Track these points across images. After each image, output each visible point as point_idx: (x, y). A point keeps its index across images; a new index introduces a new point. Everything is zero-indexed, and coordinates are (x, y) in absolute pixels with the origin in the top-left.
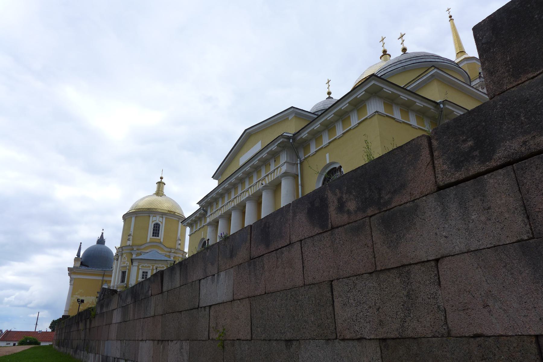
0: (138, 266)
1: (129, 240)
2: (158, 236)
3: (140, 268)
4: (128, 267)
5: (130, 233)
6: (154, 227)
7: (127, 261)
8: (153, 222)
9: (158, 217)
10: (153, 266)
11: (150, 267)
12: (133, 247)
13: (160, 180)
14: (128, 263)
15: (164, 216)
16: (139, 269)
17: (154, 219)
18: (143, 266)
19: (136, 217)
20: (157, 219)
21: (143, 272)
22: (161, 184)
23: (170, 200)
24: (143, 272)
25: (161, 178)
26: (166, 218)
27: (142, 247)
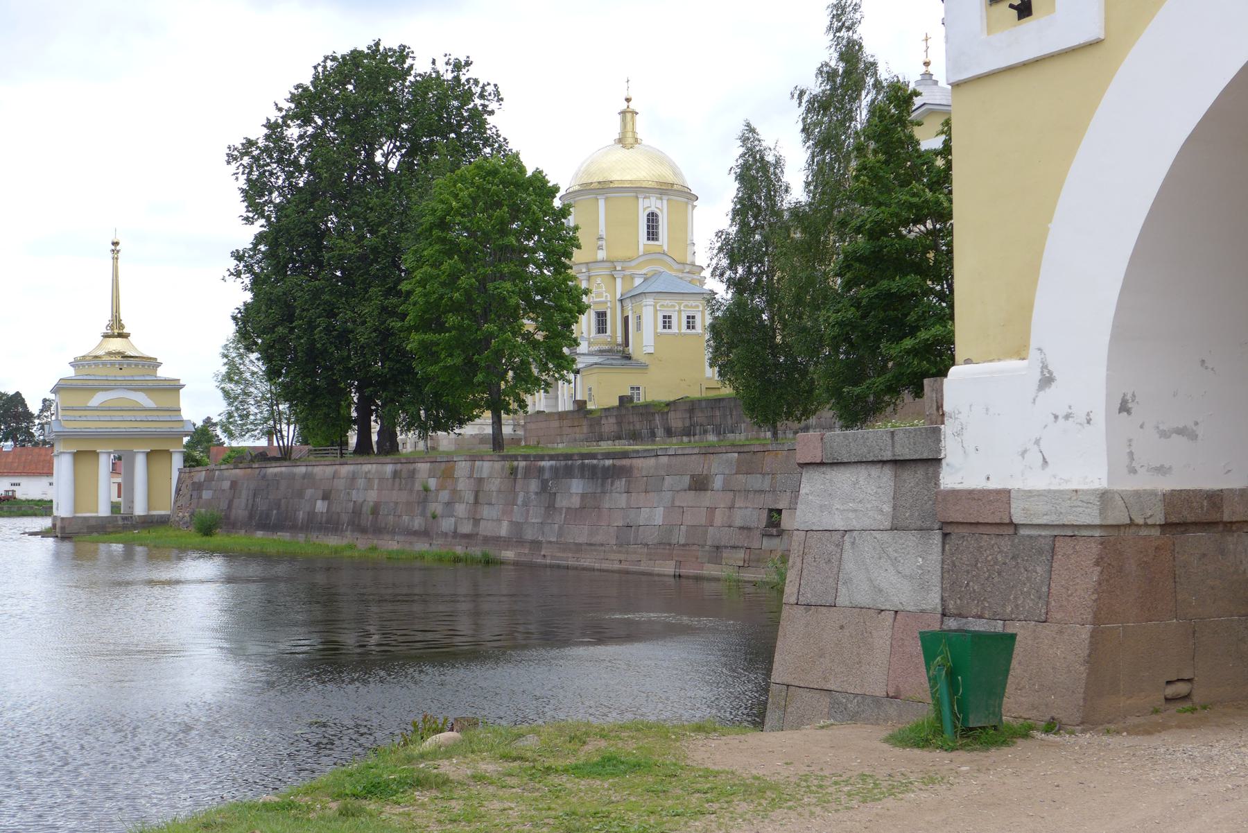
0: (655, 306)
1: (600, 248)
2: (657, 239)
3: (658, 308)
4: (609, 304)
5: (600, 233)
6: (648, 220)
7: (606, 292)
8: (645, 209)
9: (653, 199)
10: (680, 304)
11: (673, 306)
12: (616, 264)
13: (624, 105)
14: (609, 295)
15: (665, 197)
16: (656, 311)
17: (647, 202)
18: (686, 306)
19: (606, 199)
20: (652, 204)
21: (665, 317)
22: (627, 115)
23: (660, 158)
24: (665, 317)
25: (628, 100)
26: (668, 200)
27: (633, 264)
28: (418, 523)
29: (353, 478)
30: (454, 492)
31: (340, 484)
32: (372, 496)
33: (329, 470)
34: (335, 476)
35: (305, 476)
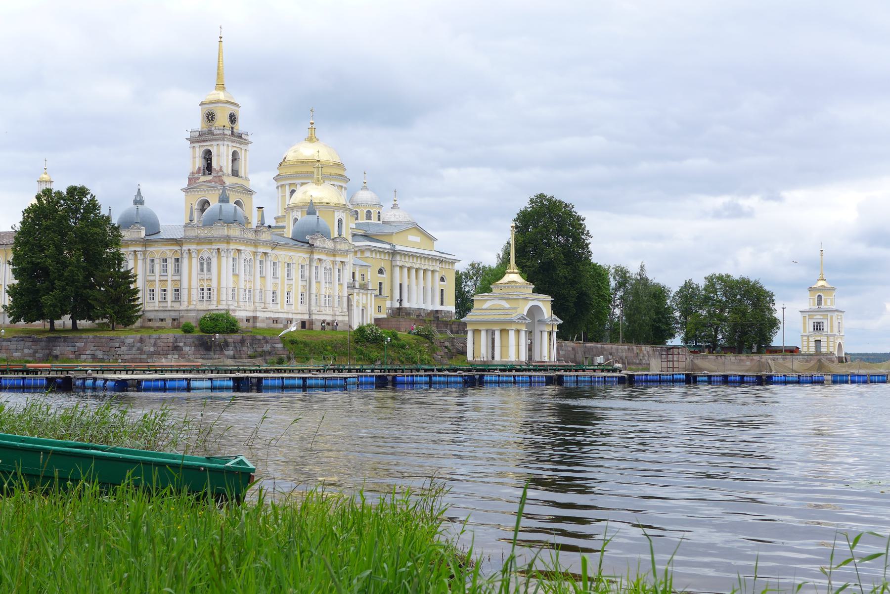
28: (638, 362)
29: (617, 349)
30: (643, 354)
31: (614, 351)
32: (624, 354)
33: (609, 346)
34: (612, 348)
35: (601, 347)
